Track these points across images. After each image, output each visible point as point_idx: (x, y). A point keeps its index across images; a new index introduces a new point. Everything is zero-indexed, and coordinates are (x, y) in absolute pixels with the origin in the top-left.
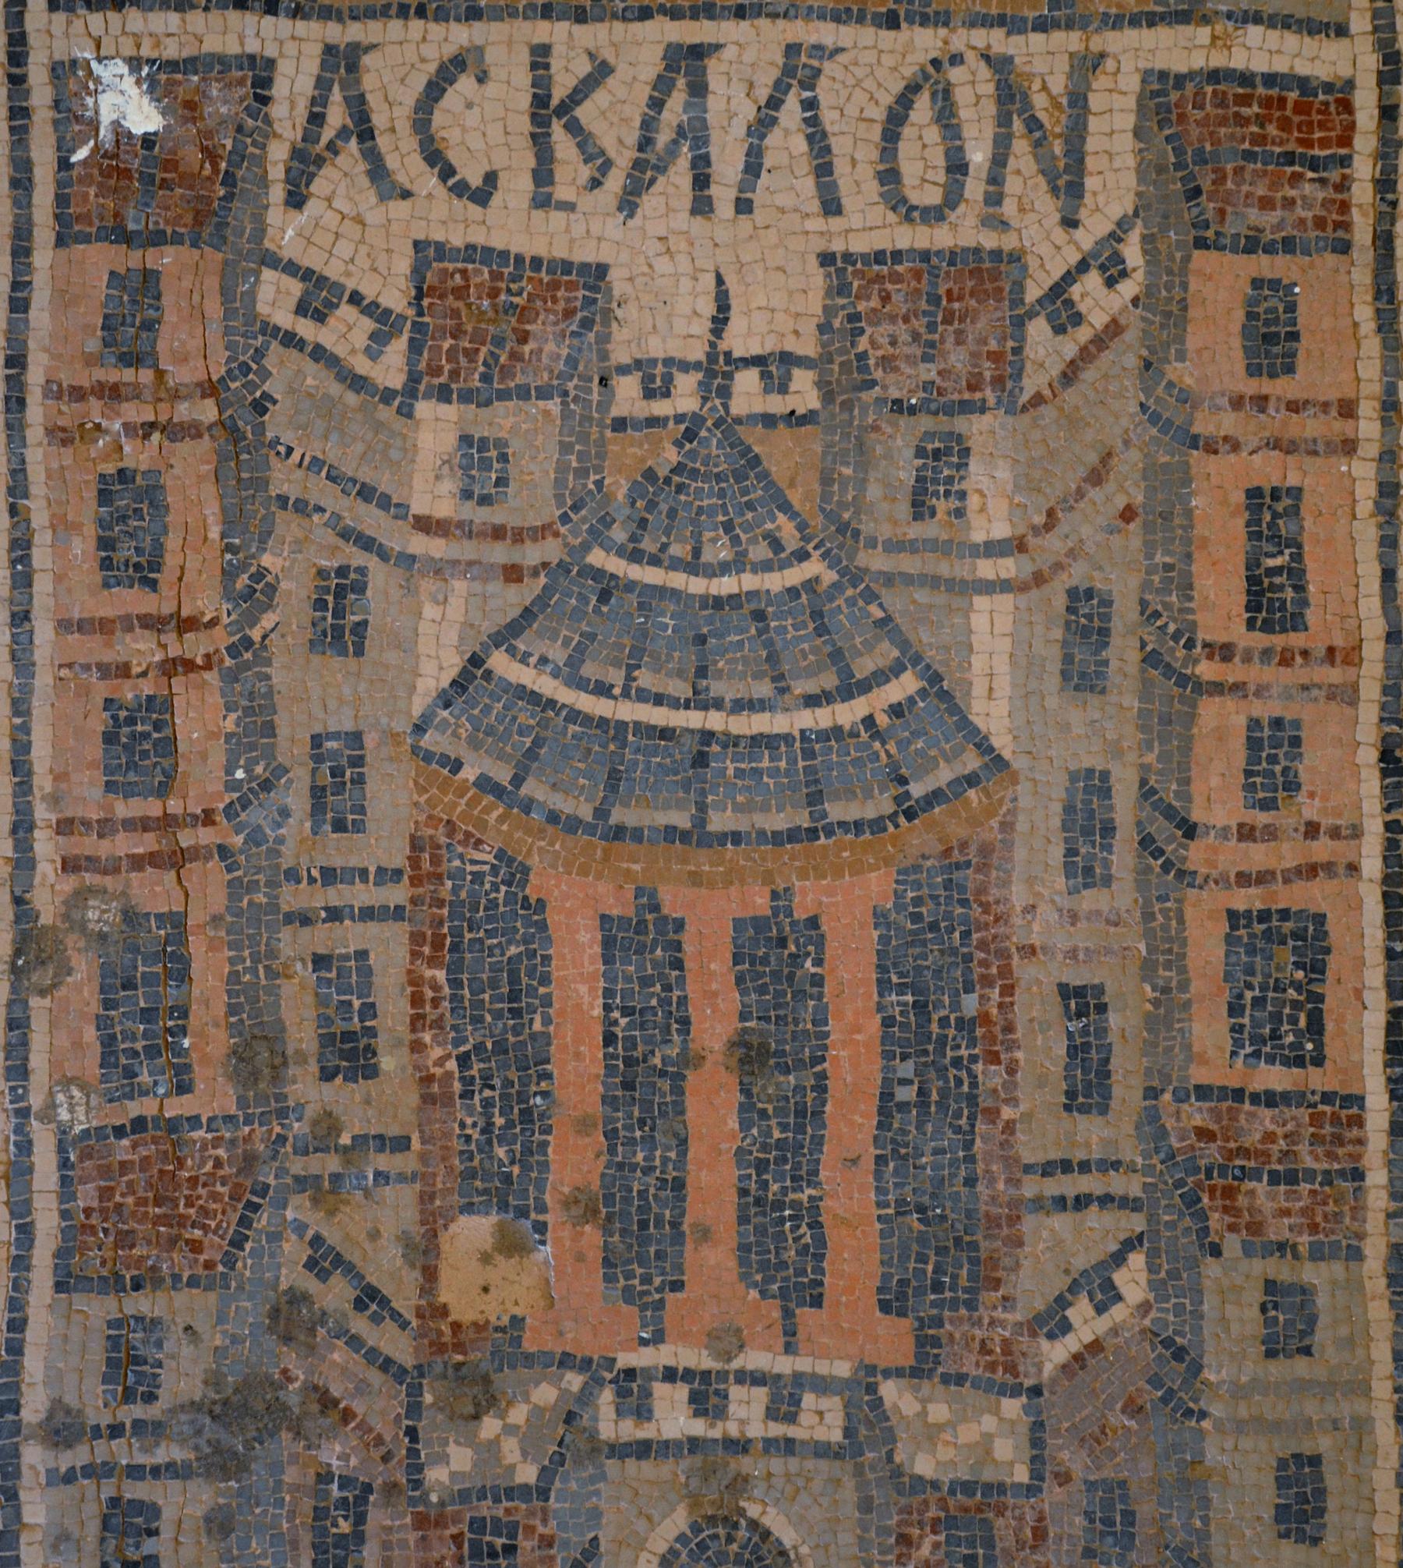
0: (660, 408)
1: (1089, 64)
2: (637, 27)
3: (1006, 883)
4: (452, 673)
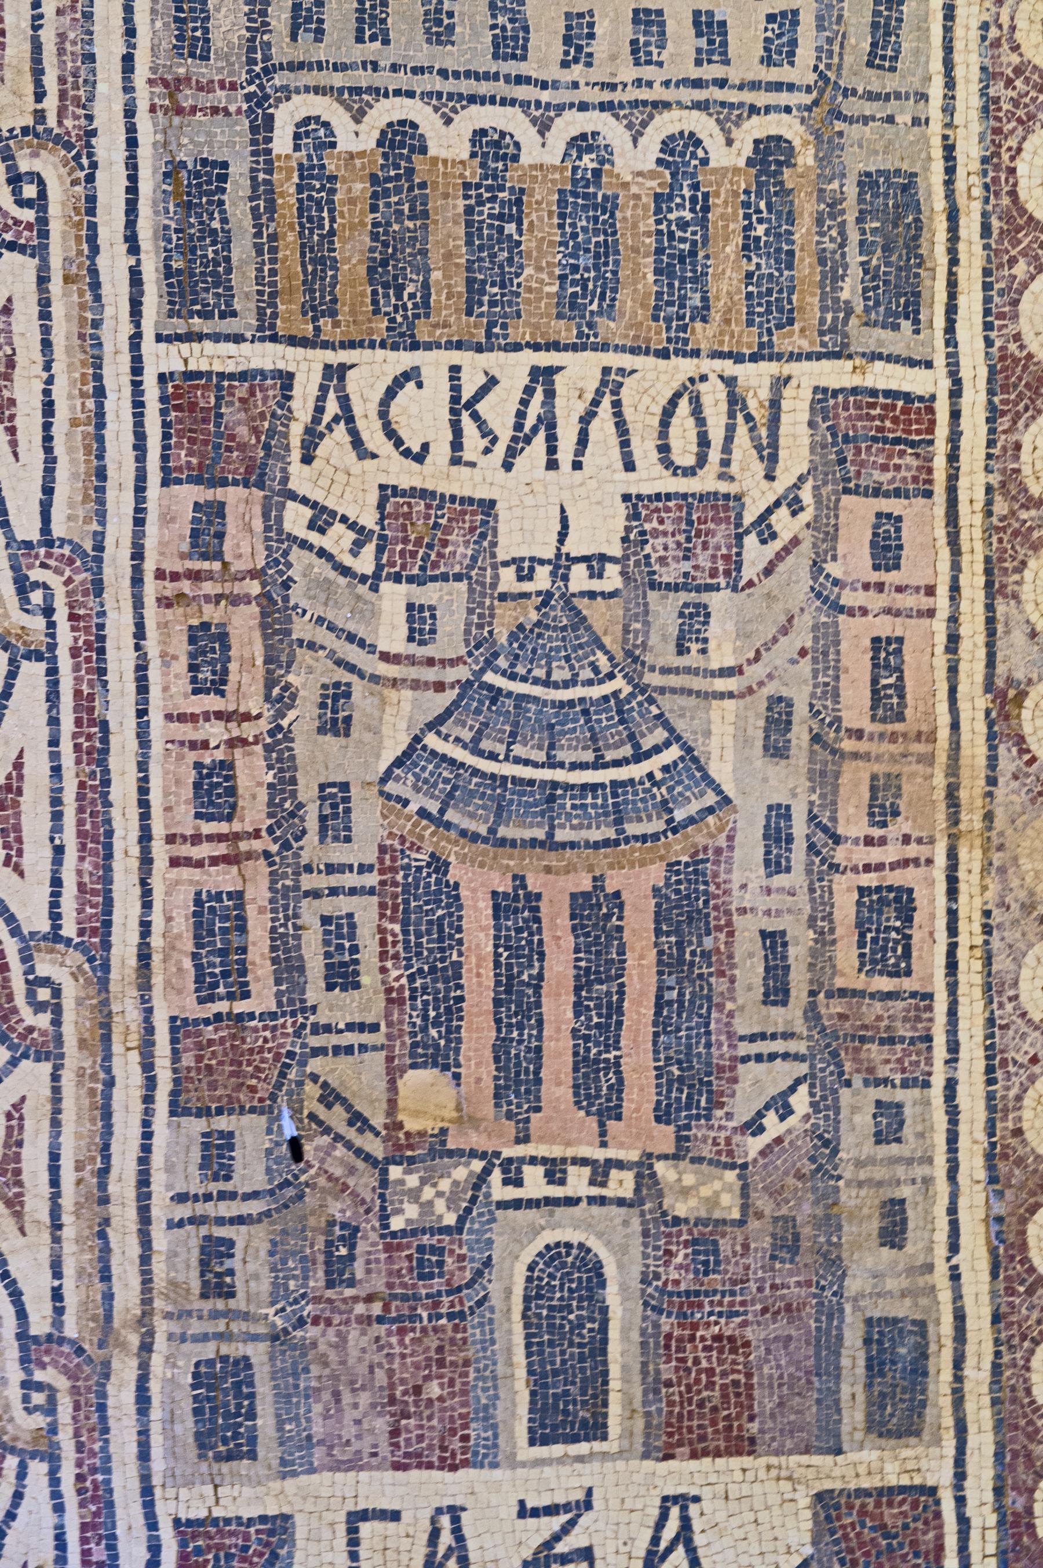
0: (527, 587)
1: (781, 383)
2: (512, 355)
3: (729, 871)
4: (403, 747)
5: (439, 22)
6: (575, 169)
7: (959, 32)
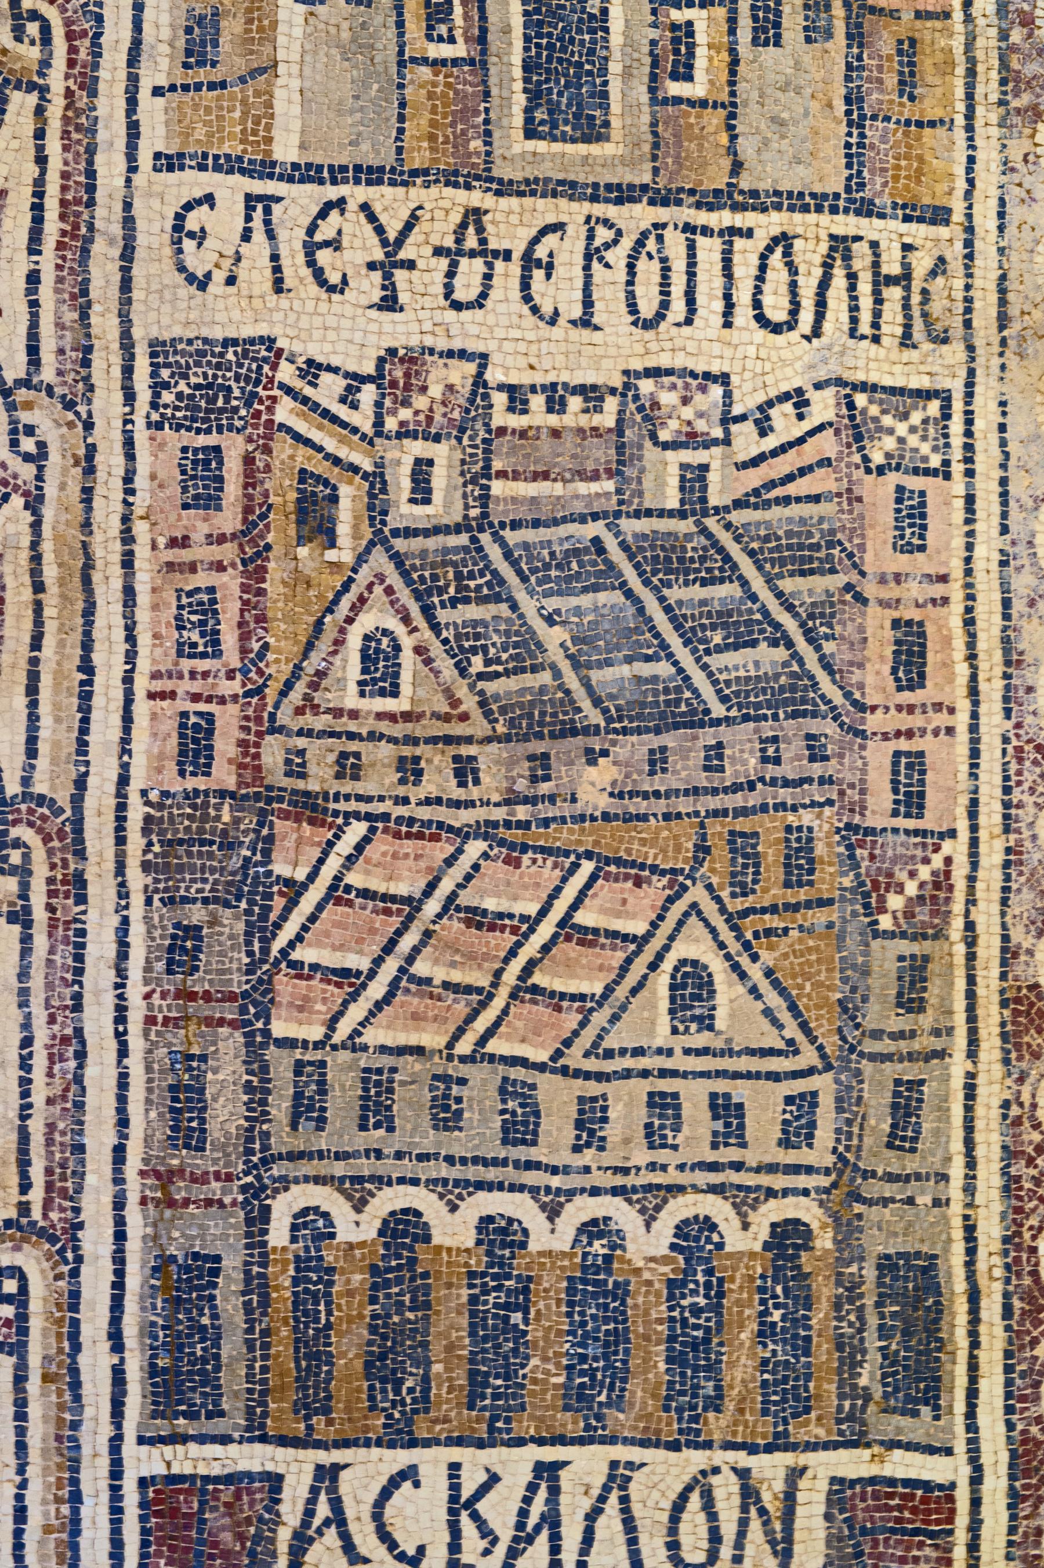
1: (795, 1474)
5: (446, 1108)
6: (585, 1255)
7: (980, 1111)
